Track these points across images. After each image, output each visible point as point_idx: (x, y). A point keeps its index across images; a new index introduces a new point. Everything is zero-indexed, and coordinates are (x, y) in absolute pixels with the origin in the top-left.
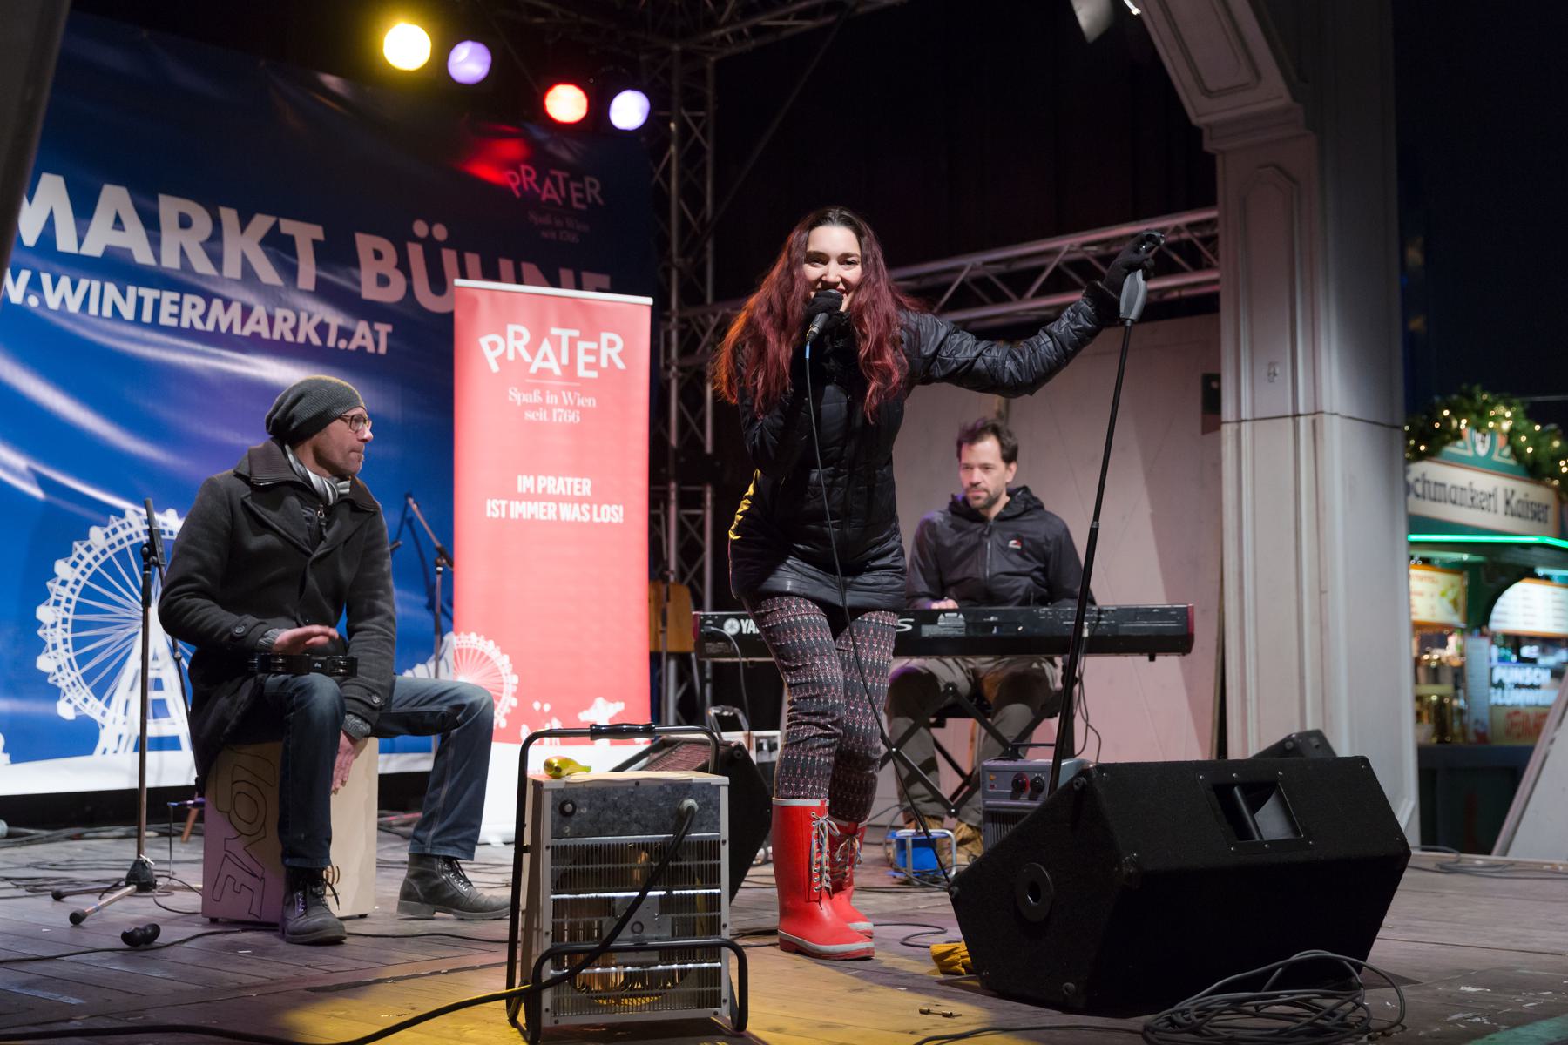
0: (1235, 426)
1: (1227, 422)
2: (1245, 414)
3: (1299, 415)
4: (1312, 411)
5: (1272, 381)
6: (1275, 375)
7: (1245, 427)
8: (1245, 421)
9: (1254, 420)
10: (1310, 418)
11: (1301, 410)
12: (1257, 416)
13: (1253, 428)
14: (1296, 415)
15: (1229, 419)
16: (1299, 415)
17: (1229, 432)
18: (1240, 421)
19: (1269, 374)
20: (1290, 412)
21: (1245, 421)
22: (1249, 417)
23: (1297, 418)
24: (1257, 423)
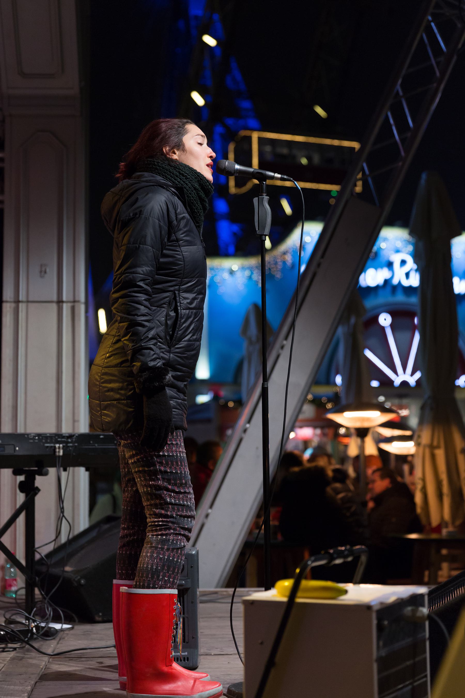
0: (13, 305)
1: (7, 302)
2: (22, 297)
3: (63, 302)
4: (72, 299)
5: (42, 277)
6: (45, 272)
7: (22, 307)
8: (22, 302)
9: (28, 302)
10: (70, 305)
11: (64, 299)
12: (31, 299)
13: (27, 306)
14: (60, 302)
15: (8, 299)
16: (63, 302)
17: (8, 309)
18: (17, 302)
19: (41, 272)
20: (55, 298)
21: (22, 302)
22: (24, 299)
23: (61, 304)
24: (30, 304)
